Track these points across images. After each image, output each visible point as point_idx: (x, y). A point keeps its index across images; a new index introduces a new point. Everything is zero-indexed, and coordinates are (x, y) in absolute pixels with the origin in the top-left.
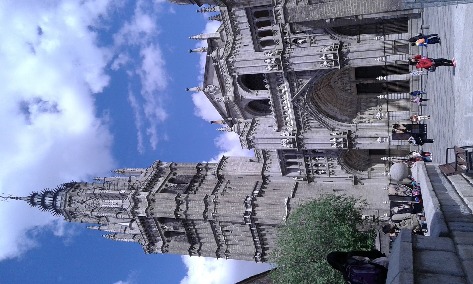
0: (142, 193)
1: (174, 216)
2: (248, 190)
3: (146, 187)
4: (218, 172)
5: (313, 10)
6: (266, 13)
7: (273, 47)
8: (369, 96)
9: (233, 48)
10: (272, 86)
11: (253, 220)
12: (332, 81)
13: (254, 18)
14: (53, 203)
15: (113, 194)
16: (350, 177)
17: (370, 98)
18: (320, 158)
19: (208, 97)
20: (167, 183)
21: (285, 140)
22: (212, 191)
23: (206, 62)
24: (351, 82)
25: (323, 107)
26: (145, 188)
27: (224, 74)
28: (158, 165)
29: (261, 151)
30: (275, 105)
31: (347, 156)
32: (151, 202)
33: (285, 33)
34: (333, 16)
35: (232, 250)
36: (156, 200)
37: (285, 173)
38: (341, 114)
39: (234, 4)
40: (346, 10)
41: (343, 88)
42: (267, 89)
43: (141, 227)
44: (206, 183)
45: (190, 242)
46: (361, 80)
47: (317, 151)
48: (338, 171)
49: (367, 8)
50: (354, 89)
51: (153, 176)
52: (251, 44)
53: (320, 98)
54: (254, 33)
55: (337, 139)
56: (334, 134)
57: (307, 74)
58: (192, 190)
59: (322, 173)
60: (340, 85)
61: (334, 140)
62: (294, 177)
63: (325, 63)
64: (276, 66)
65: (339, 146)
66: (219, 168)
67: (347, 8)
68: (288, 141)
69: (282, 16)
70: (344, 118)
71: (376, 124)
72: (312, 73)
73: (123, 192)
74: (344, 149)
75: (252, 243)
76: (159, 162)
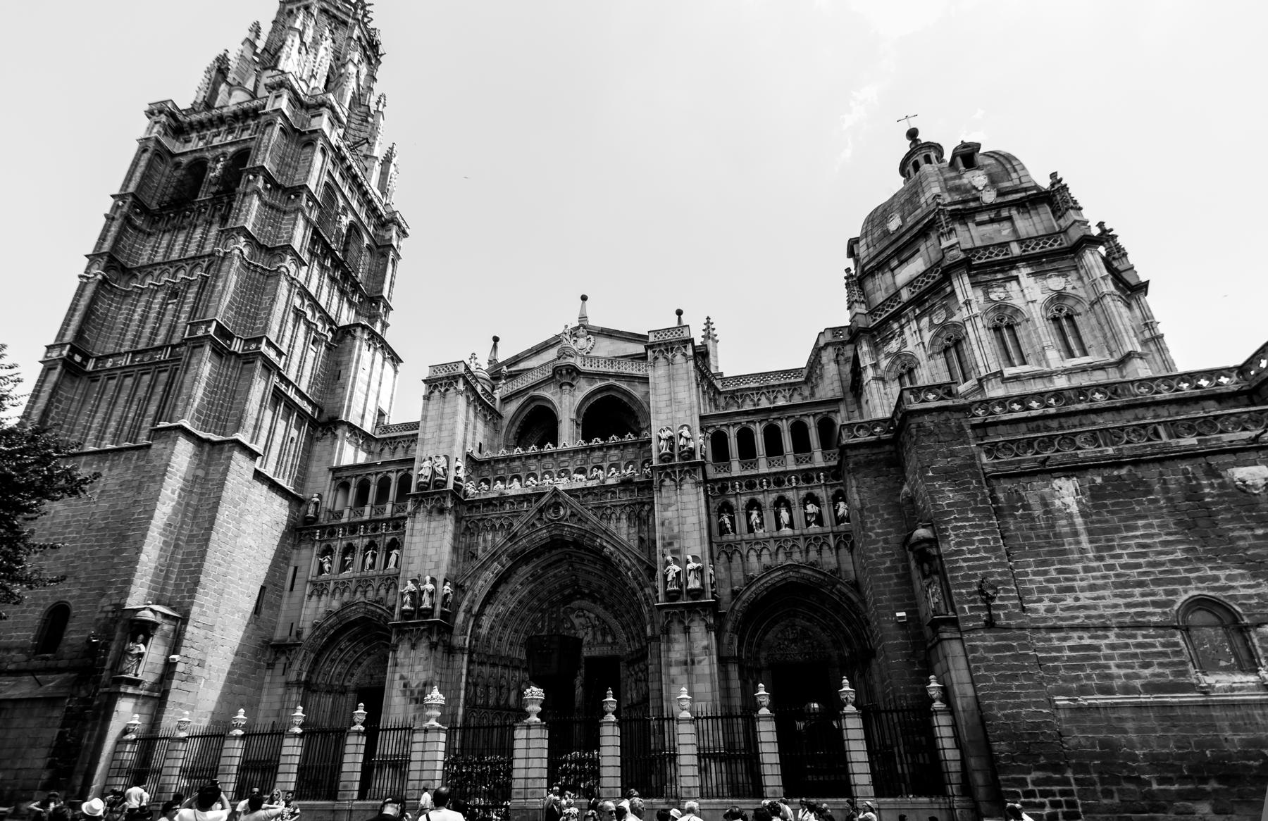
5: (968, 489)
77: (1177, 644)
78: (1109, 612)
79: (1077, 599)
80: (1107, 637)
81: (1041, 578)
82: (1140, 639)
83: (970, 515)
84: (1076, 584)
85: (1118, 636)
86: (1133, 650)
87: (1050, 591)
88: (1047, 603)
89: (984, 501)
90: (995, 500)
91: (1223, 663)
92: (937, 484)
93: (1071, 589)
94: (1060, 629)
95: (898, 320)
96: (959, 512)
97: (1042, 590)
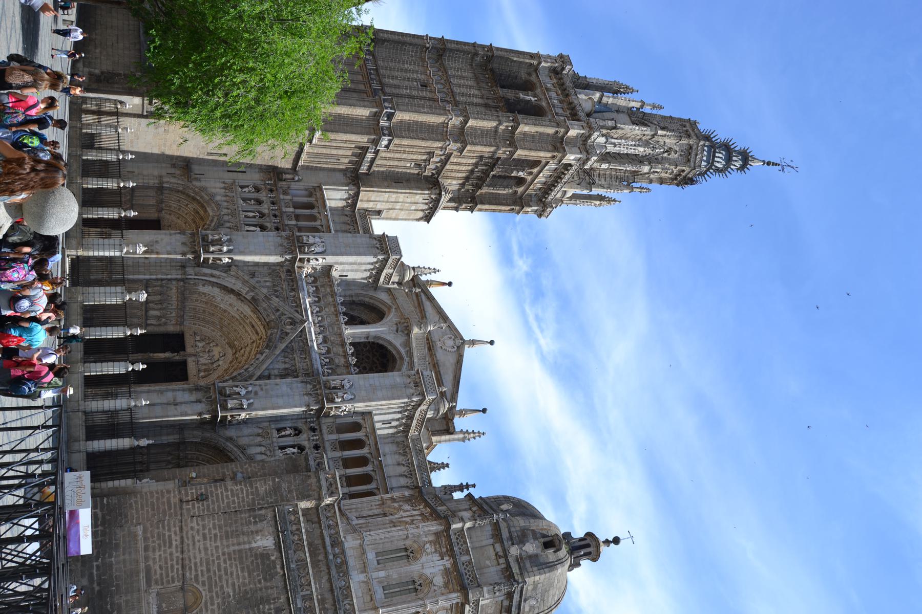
0: (573, 163)
1: (520, 117)
2: (385, 158)
4: (440, 195)
6: (350, 481)
7: (339, 421)
8: (161, 329)
9: (410, 418)
10: (340, 350)
11: (380, 106)
12: (230, 357)
13: (373, 474)
14: (715, 152)
15: (620, 163)
16: (196, 179)
17: (160, 325)
18: (251, 214)
19: (456, 329)
20: (529, 178)
22: (452, 159)
23: (457, 392)
24: (195, 355)
25: (247, 310)
26: (568, 170)
27: (429, 373)
28: (543, 211)
29: (361, 231)
31: (202, 219)
32: (558, 145)
33: (316, 447)
34: (229, 484)
35: (417, 52)
36: (550, 148)
37: (317, 189)
38: (213, 297)
39: (410, 500)
41: (209, 343)
42: (351, 344)
43: (576, 102)
44: (460, 175)
45: (492, 70)
46: (177, 358)
47: (258, 229)
48: (218, 190)
49: (165, 500)
50: (189, 341)
51: (552, 191)
52: (377, 425)
53: (253, 326)
54: (373, 447)
55: (220, 250)
57: (276, 372)
58: (485, 165)
59: (248, 186)
60: (214, 348)
62: (299, 181)
63: (243, 392)
64: (335, 388)
65: (217, 237)
69: (324, 484)
70: (207, 289)
71: (148, 277)
72: (266, 373)
73: (605, 166)
74: (208, 232)
75: (380, 63)
76: (540, 216)
77: (173, 582)
78: (191, 554)
79: (199, 541)
81: (211, 526)
82: (176, 567)
84: (208, 541)
85: (178, 557)
87: (204, 529)
88: (196, 527)
89: (259, 504)
90: (260, 509)
91: (164, 605)
92: (271, 483)
93: (205, 538)
94: (181, 529)
95: (425, 507)
96: (252, 493)
97: (204, 527)
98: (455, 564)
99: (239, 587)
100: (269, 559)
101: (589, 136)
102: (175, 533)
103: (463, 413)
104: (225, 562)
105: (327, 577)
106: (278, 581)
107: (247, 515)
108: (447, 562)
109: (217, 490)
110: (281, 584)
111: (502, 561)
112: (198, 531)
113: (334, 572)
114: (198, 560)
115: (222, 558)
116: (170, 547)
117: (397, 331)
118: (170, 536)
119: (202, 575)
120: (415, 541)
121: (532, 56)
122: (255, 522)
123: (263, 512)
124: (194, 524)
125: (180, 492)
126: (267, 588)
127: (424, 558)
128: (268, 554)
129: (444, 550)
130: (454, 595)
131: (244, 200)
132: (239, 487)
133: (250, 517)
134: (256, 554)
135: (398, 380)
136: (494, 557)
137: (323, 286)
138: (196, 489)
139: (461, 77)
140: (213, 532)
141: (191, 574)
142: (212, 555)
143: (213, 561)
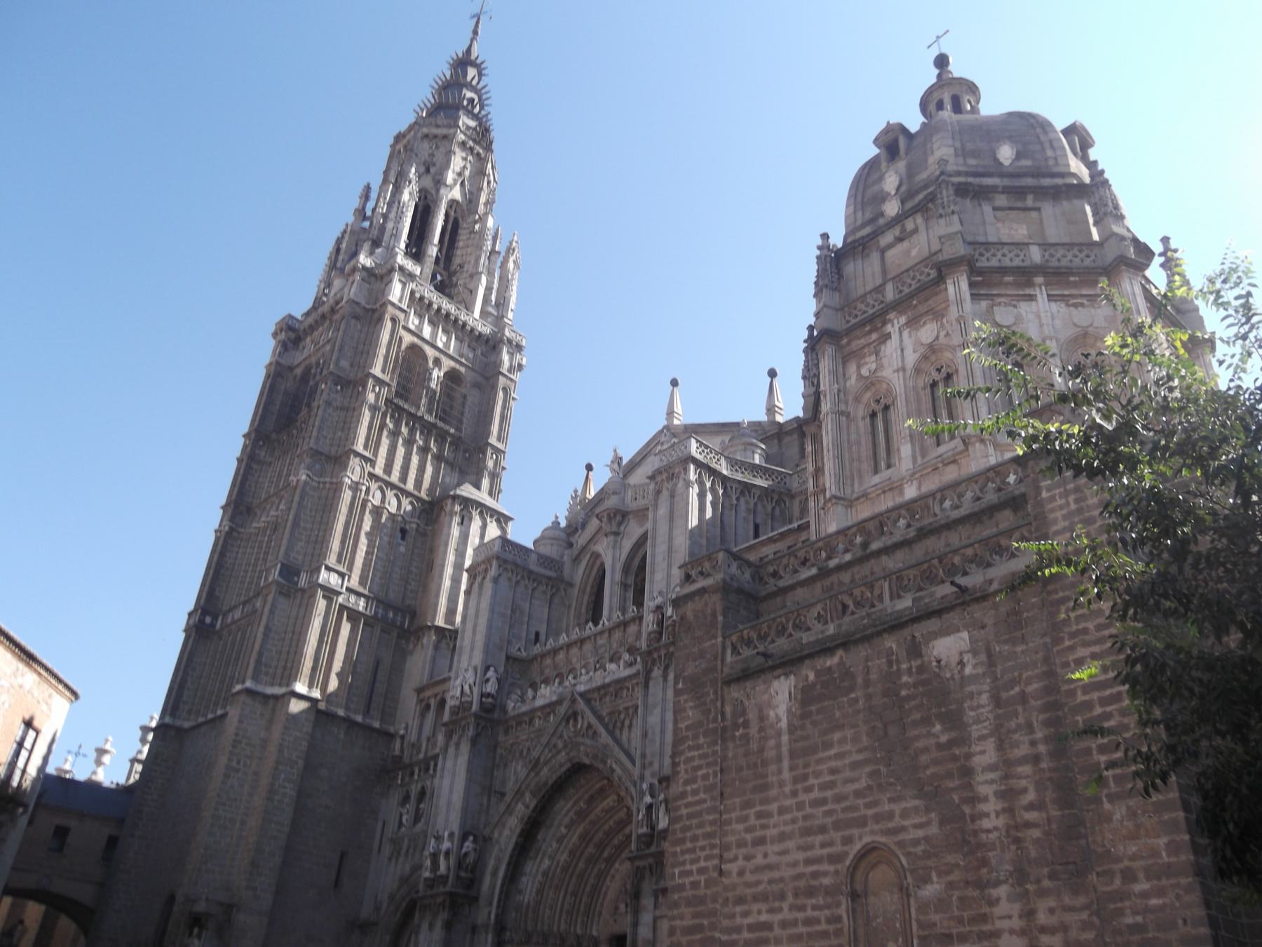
3: (435, 307)
9: (746, 488)
10: (632, 629)
20: (447, 364)
21: (471, 681)
22: (395, 477)
25: (565, 809)
28: (510, 341)
30: (582, 641)
32: (376, 315)
34: (676, 789)
37: (422, 696)
38: (545, 874)
40: (689, 845)
51: (472, 330)
53: (592, 798)
55: (447, 853)
56: (468, 845)
59: (401, 816)
61: (446, 845)
64: (660, 623)
65: (428, 862)
66: (467, 503)
67: (693, 850)
68: (466, 688)
76: (519, 348)
77: (838, 919)
78: (788, 873)
80: (781, 909)
81: (740, 827)
82: (810, 913)
83: (702, 740)
85: (791, 908)
86: (802, 929)
89: (715, 720)
90: (723, 714)
93: (761, 841)
94: (741, 900)
97: (741, 844)
98: (898, 306)
99: (860, 751)
100: (814, 685)
101: (364, 268)
102: (745, 914)
103: (771, 409)
104: (808, 790)
105: (884, 558)
106: (855, 658)
107: (731, 745)
108: (896, 324)
109: (681, 816)
110: (862, 651)
111: (910, 225)
112: (748, 858)
113: (875, 546)
114: (801, 856)
115: (803, 797)
116: (767, 926)
117: (616, 534)
118: (751, 928)
119: (830, 844)
120: (857, 399)
121: (268, 376)
122: (746, 724)
123: (728, 709)
124: (733, 868)
125: (676, 905)
126: (867, 683)
127: (887, 373)
128: (802, 690)
129: (874, 336)
130: (951, 289)
131: (417, 818)
132: (682, 767)
133: (734, 737)
134: (804, 716)
135: (662, 511)
136: (906, 244)
137: (542, 673)
138: (673, 866)
139: (280, 476)
140: (753, 821)
141: (825, 874)
142: (794, 821)
143: (805, 818)
